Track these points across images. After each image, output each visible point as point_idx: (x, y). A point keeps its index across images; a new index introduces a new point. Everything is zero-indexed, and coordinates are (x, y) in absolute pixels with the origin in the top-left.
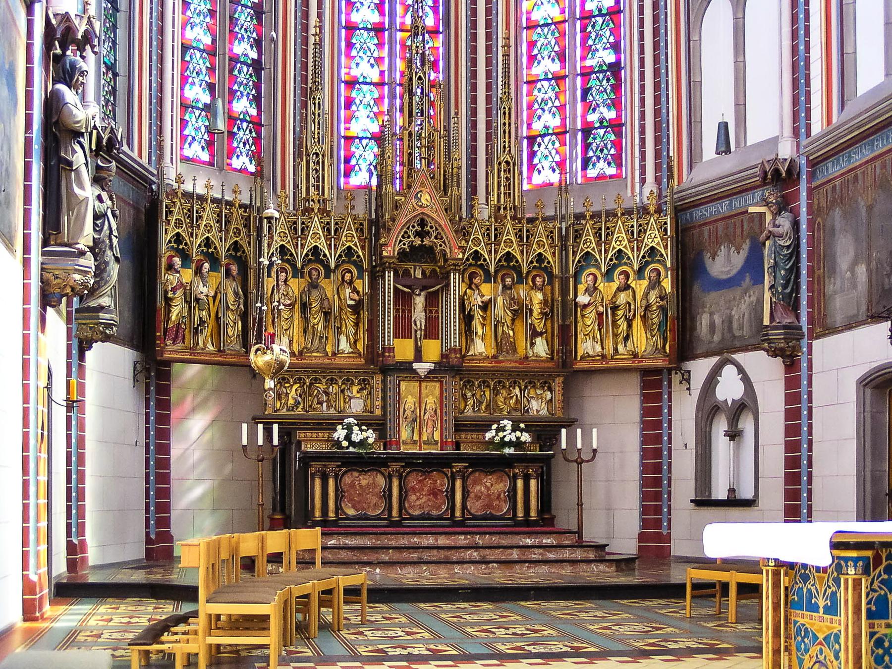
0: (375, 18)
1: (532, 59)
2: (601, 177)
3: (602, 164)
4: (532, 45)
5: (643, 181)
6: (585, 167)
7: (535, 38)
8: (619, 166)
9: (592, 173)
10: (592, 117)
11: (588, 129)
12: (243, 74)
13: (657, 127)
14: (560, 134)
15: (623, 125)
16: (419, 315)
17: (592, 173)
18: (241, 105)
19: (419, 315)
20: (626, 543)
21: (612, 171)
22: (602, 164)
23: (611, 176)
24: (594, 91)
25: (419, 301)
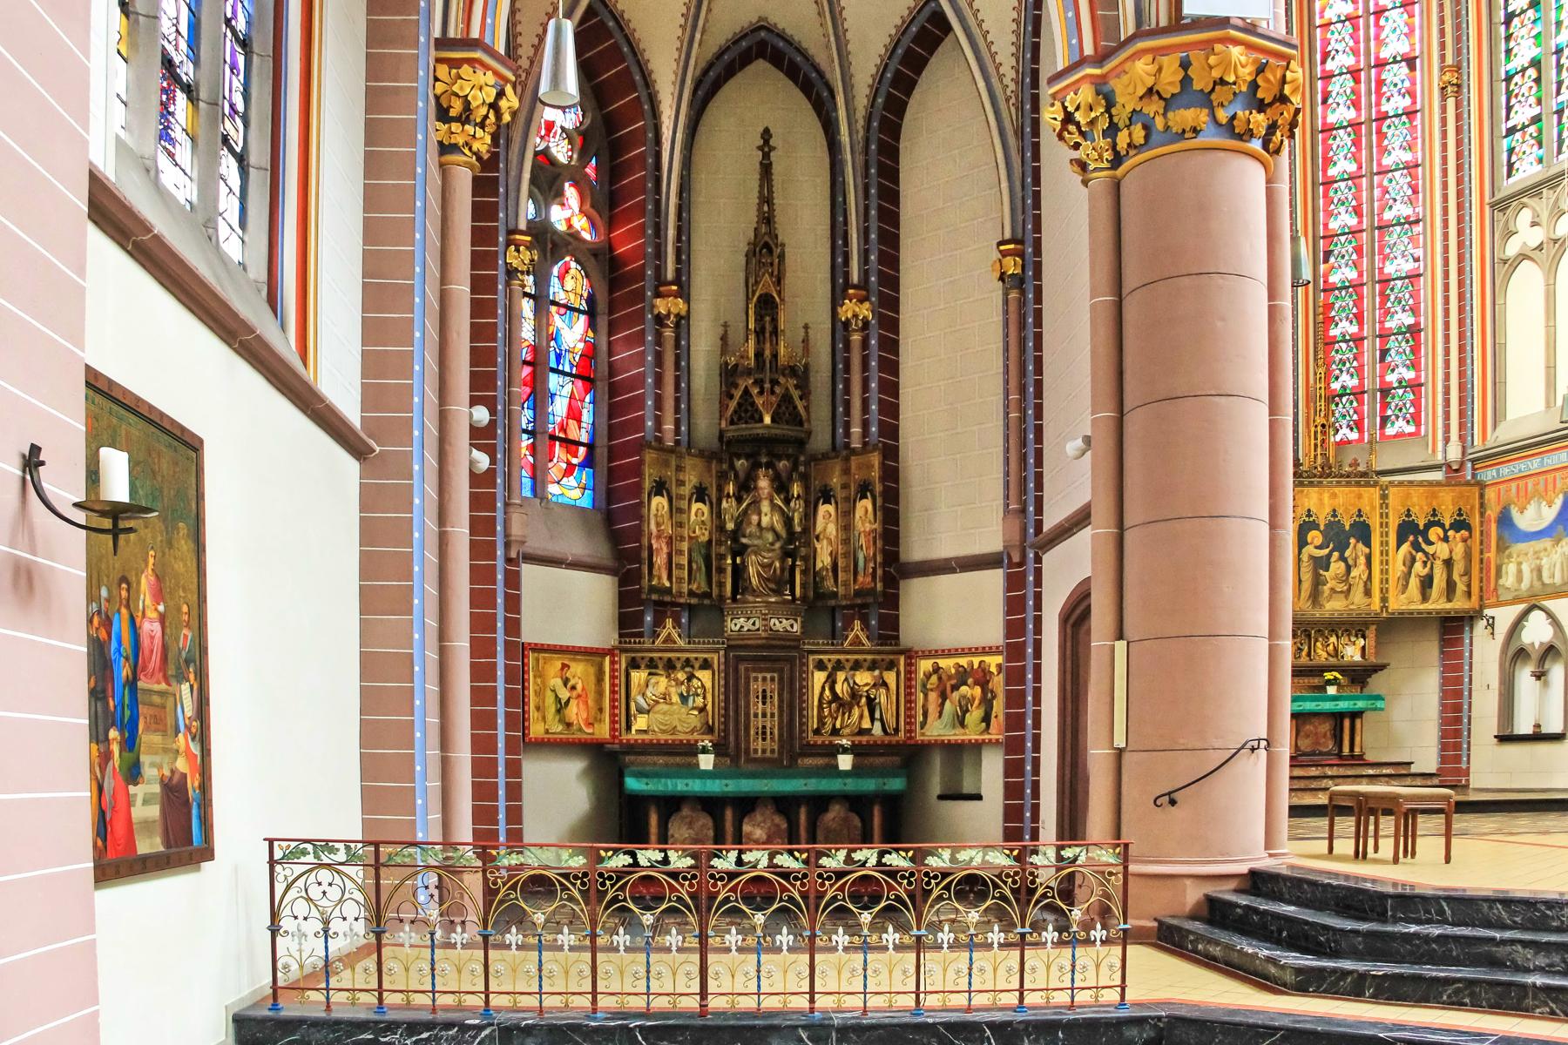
2: (1399, 435)
3: (1401, 423)
5: (1447, 440)
6: (1383, 426)
7: (1332, 300)
8: (1418, 424)
10: (1391, 378)
11: (1386, 391)
13: (1462, 387)
14: (1358, 393)
15: (1421, 385)
17: (1390, 431)
21: (1411, 429)
22: (1401, 423)
23: (1410, 434)
24: (1393, 352)
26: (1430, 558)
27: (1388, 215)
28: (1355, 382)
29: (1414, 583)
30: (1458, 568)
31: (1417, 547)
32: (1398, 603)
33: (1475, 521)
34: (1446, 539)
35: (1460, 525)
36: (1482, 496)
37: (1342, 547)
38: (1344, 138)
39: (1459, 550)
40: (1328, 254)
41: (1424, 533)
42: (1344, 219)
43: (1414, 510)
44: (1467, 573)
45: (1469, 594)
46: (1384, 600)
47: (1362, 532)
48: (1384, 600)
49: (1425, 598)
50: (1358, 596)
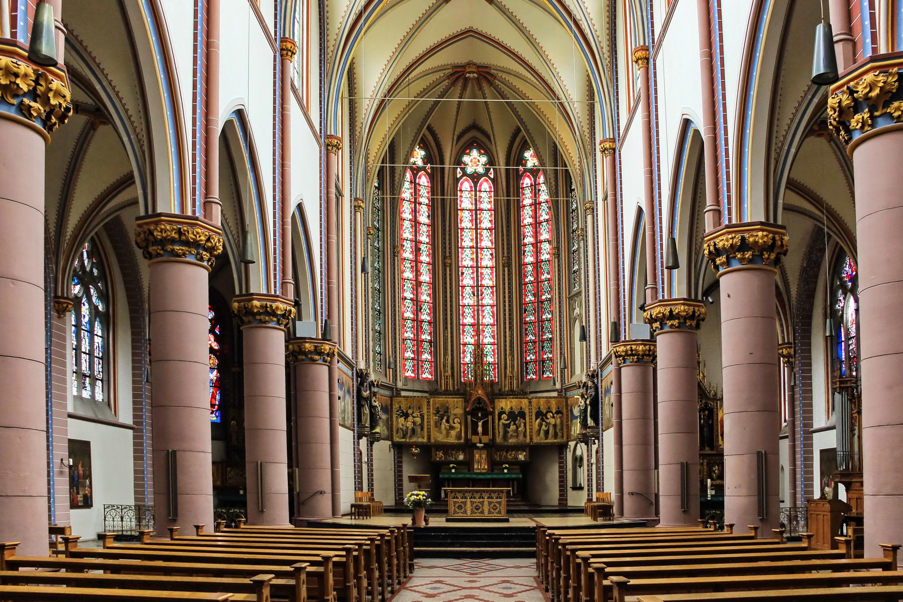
0: (472, 321)
1: (526, 334)
4: (526, 330)
9: (545, 376)
11: (544, 361)
12: (426, 345)
14: (535, 361)
16: (480, 429)
17: (545, 376)
18: (426, 356)
19: (480, 429)
20: (556, 503)
25: (480, 424)
26: (548, 424)
27: (544, 297)
28: (533, 357)
29: (542, 433)
30: (558, 427)
31: (543, 420)
32: (536, 440)
33: (564, 411)
34: (553, 417)
35: (558, 412)
36: (567, 402)
37: (514, 420)
38: (530, 268)
39: (558, 421)
40: (526, 310)
41: (546, 415)
42: (530, 298)
43: (542, 407)
44: (562, 429)
45: (563, 437)
46: (531, 439)
47: (522, 415)
48: (531, 439)
49: (546, 438)
50: (521, 437)
